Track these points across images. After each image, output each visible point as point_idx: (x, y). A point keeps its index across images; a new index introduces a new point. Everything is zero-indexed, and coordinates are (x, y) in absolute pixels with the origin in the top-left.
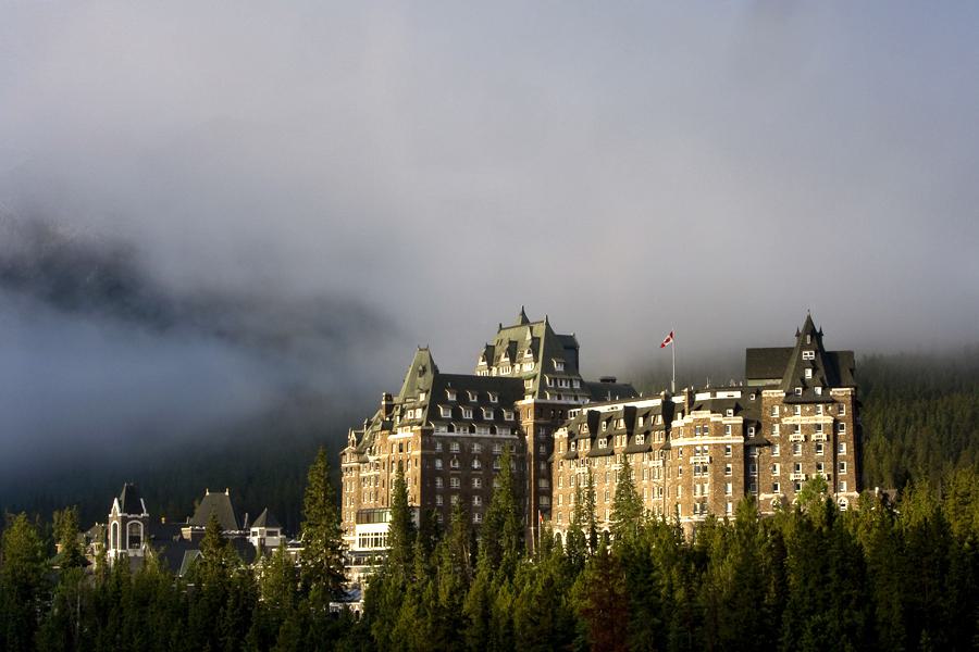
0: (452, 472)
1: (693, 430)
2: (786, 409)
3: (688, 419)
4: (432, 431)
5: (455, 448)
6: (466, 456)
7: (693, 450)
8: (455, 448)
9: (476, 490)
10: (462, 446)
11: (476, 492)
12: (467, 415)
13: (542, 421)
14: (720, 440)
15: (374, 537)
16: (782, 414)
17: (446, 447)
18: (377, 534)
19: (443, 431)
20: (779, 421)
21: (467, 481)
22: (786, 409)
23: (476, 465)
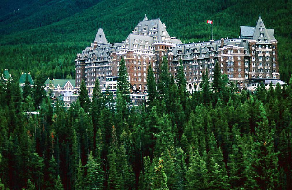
0: (139, 65)
2: (257, 46)
4: (133, 52)
5: (139, 58)
9: (145, 71)
10: (141, 57)
11: (145, 72)
13: (162, 50)
14: (236, 55)
15: (114, 85)
16: (255, 47)
17: (137, 57)
18: (115, 85)
20: (255, 50)
21: (142, 69)
22: (257, 46)
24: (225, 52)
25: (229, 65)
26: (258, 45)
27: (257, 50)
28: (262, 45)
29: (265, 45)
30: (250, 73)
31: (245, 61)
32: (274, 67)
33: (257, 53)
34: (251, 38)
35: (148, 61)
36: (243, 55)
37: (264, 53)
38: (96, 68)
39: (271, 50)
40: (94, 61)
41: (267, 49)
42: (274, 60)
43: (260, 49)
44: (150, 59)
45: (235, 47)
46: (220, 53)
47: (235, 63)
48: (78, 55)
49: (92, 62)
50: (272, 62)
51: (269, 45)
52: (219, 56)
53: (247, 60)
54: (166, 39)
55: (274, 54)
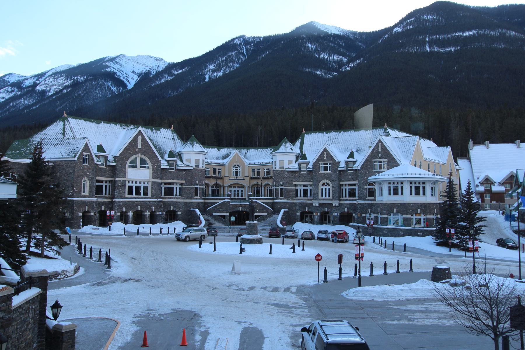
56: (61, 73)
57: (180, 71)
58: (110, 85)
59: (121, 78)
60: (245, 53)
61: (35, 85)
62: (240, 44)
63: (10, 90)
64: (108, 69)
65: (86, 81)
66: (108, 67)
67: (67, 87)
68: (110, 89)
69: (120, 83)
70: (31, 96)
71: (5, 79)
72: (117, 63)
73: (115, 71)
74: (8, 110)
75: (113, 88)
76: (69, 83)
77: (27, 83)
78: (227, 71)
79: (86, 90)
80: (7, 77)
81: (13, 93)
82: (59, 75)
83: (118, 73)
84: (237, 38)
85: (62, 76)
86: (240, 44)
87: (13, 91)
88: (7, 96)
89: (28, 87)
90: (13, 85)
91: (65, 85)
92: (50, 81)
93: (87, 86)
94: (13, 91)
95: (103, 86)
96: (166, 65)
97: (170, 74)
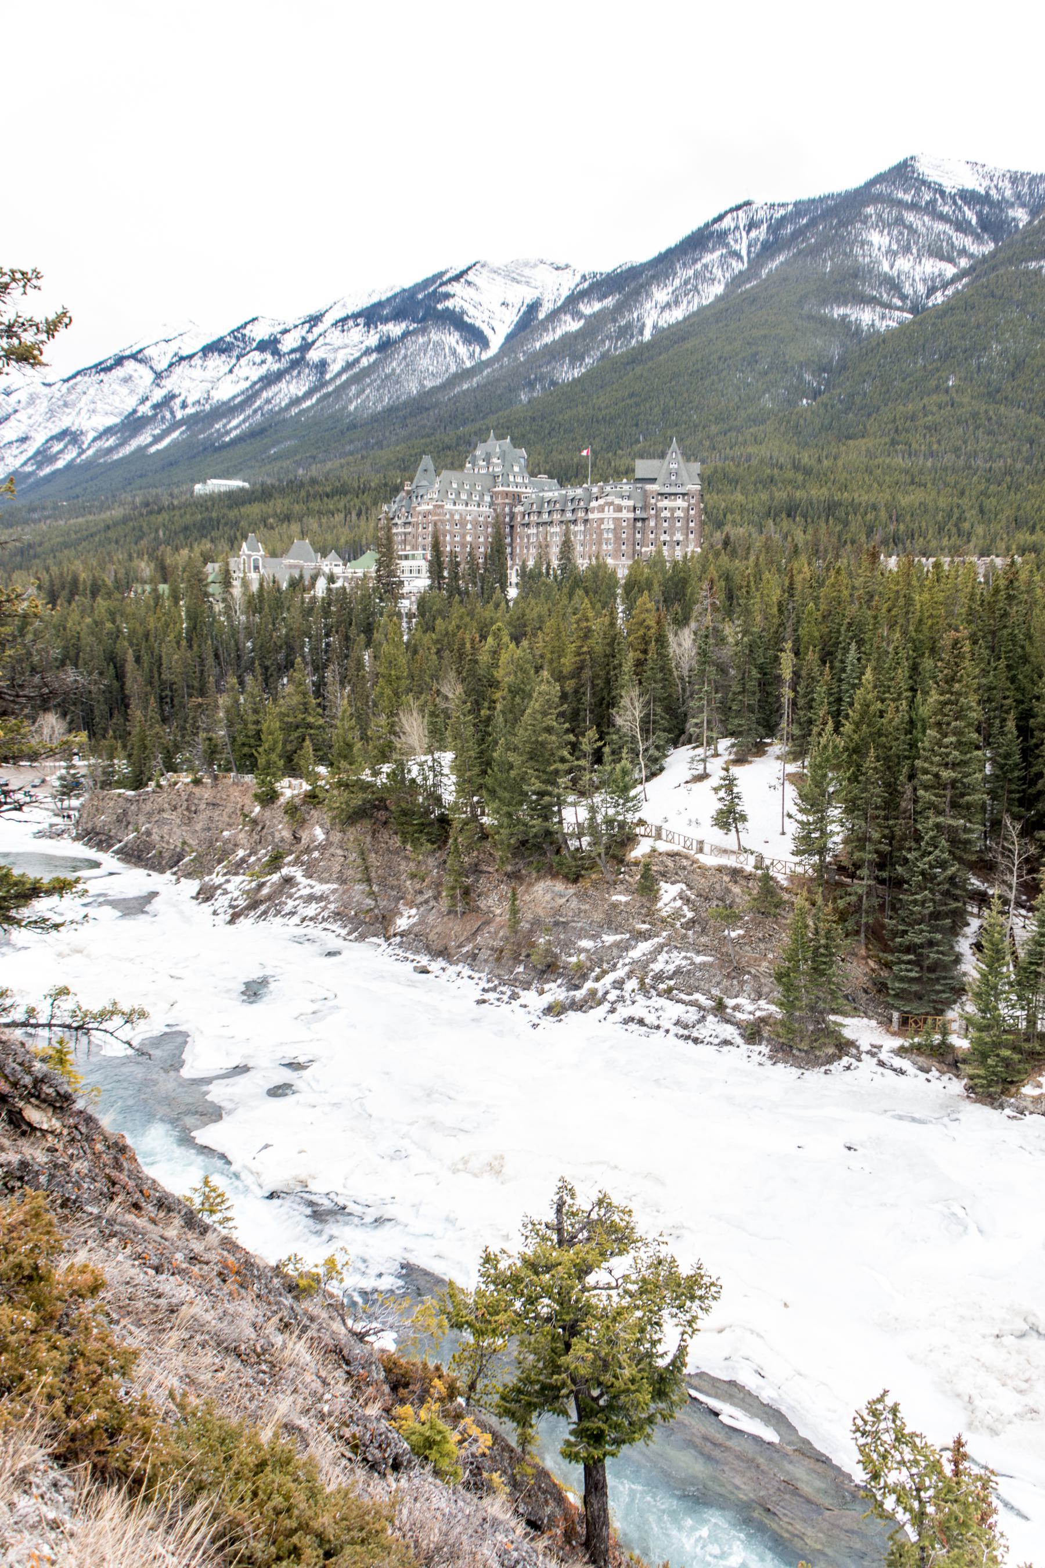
1: (601, 509)
3: (601, 501)
6: (463, 523)
7: (602, 520)
8: (457, 517)
12: (464, 497)
17: (452, 515)
19: (449, 506)
21: (463, 536)
23: (469, 526)
24: (601, 509)
25: (605, 536)
26: (661, 494)
27: (660, 504)
28: (671, 494)
29: (675, 494)
30: (644, 550)
31: (634, 527)
32: (691, 536)
33: (659, 511)
34: (653, 480)
35: (476, 524)
36: (631, 515)
37: (673, 510)
38: (405, 534)
39: (685, 504)
40: (403, 520)
41: (680, 502)
42: (692, 525)
43: (666, 503)
44: (481, 519)
45: (618, 501)
46: (593, 510)
47: (615, 531)
48: (385, 508)
49: (399, 522)
50: (688, 527)
51: (684, 495)
52: (591, 516)
53: (639, 524)
54: (519, 480)
55: (692, 512)
56: (355, 316)
57: (597, 306)
58: (454, 344)
59: (478, 323)
60: (744, 253)
61: (306, 346)
62: (737, 228)
63: (258, 360)
64: (449, 304)
65: (406, 334)
66: (447, 296)
67: (368, 352)
68: (454, 353)
69: (474, 335)
70: (299, 373)
71: (246, 332)
72: (469, 283)
73: (466, 306)
74: (260, 408)
75: (462, 350)
76: (373, 340)
77: (289, 343)
78: (694, 307)
79: (405, 357)
80: (249, 327)
81: (265, 367)
82: (351, 323)
83: (471, 311)
84: (731, 210)
85: (357, 325)
86: (737, 228)
87: (263, 362)
88: (256, 374)
89: (293, 351)
90: (263, 346)
91: (363, 347)
92: (335, 337)
93: (407, 349)
94: (263, 362)
95: (439, 345)
96: (578, 279)
97: (577, 315)
